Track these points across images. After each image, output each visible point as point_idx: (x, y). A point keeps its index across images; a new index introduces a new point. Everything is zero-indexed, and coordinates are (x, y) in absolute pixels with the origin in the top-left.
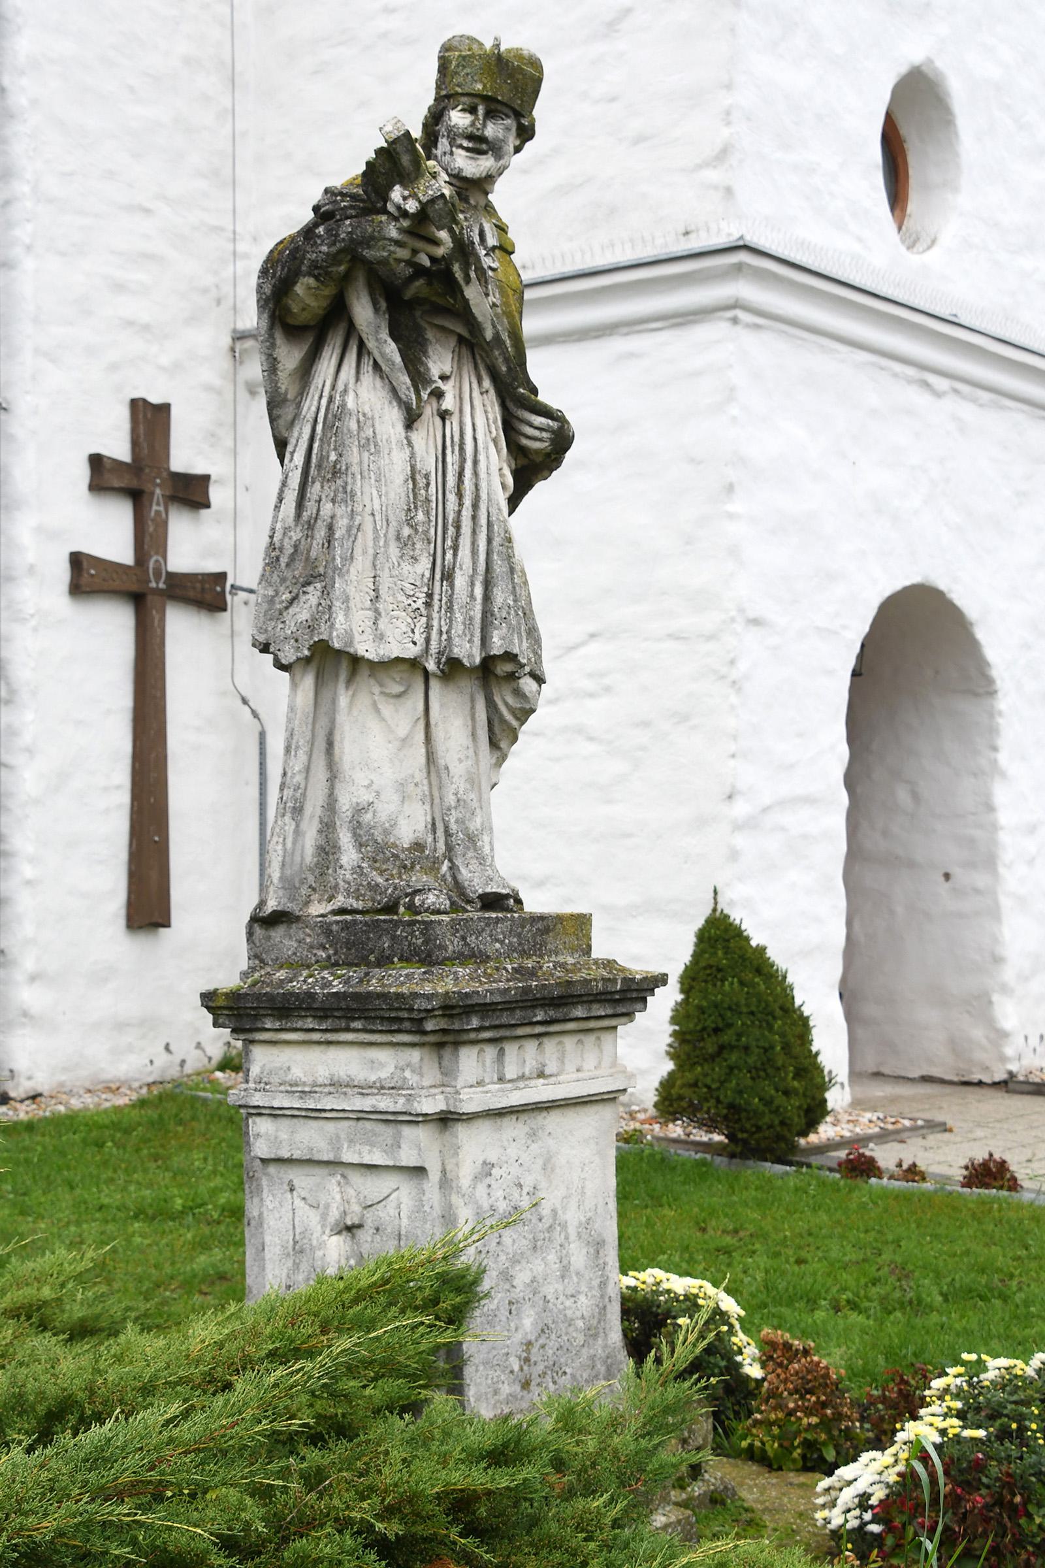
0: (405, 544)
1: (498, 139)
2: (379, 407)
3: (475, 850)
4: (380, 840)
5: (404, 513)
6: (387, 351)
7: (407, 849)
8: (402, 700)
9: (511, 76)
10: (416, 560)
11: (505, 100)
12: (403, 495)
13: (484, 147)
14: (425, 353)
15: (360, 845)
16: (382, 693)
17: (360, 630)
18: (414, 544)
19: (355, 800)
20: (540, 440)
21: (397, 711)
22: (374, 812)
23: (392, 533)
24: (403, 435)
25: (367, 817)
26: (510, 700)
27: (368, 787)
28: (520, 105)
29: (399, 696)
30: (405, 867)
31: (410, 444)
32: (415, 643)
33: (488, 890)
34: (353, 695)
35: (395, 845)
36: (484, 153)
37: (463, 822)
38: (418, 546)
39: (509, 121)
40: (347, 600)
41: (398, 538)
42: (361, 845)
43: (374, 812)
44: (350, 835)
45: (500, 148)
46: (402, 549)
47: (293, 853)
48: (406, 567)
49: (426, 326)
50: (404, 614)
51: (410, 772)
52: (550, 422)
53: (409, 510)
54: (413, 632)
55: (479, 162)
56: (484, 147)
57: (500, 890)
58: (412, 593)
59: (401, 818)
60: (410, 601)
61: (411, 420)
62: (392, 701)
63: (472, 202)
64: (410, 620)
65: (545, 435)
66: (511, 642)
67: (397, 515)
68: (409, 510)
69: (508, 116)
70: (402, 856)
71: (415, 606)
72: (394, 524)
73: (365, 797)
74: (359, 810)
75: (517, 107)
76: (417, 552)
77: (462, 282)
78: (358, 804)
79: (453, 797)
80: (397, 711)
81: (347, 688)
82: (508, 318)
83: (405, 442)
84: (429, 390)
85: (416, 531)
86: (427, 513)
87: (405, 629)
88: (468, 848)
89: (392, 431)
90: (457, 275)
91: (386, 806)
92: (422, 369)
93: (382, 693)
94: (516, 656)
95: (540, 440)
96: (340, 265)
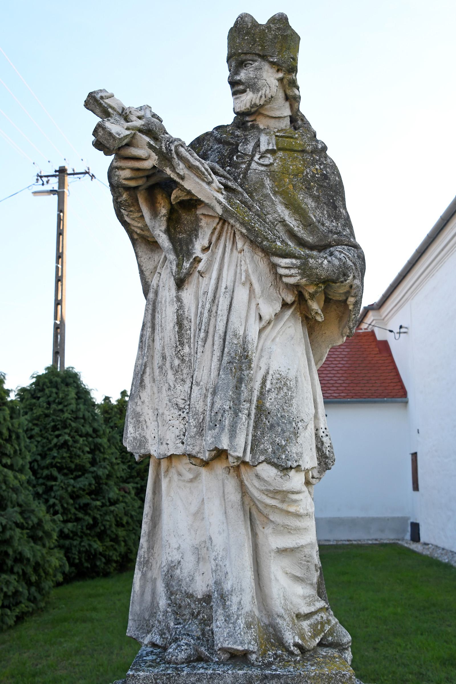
0: (177, 371)
1: (251, 79)
2: (164, 280)
3: (224, 608)
4: (183, 592)
5: (173, 349)
6: (161, 241)
7: (199, 600)
8: (195, 484)
9: (247, 34)
10: (184, 381)
11: (245, 50)
12: (173, 337)
13: (241, 87)
14: (197, 236)
15: (170, 593)
16: (179, 480)
17: (153, 436)
18: (182, 370)
19: (170, 559)
20: (291, 276)
21: (191, 493)
22: (181, 569)
23: (168, 364)
24: (175, 295)
25: (178, 572)
26: (256, 483)
27: (178, 548)
28: (261, 50)
29: (191, 481)
30: (193, 614)
31: (179, 299)
32: (183, 443)
33: (225, 645)
34: (170, 481)
35: (190, 596)
36: (244, 91)
37: (220, 584)
38: (185, 371)
39: (257, 64)
40: (137, 415)
41: (172, 368)
42: (172, 594)
43: (181, 569)
44: (164, 585)
45: (254, 84)
46: (175, 375)
47: (143, 594)
48: (179, 388)
49: (201, 217)
50: (178, 422)
51: (203, 539)
52: (294, 261)
53: (177, 347)
54: (184, 435)
55: (242, 99)
56: (241, 87)
57: (235, 647)
58: (183, 406)
59: (197, 574)
60: (181, 413)
61: (180, 283)
62: (188, 485)
63: (261, 127)
64: (182, 426)
65: (293, 271)
66: (220, 441)
67: (169, 352)
68: (177, 347)
69: (254, 61)
70: (193, 606)
71: (183, 415)
72: (168, 359)
73: (176, 556)
74: (172, 567)
75: (257, 52)
76: (185, 376)
77: (178, 180)
78: (172, 562)
79: (213, 562)
80: (191, 493)
81: (165, 476)
82: (281, 194)
83: (175, 299)
84: (191, 260)
85: (183, 361)
86: (189, 347)
87: (178, 434)
88: (218, 606)
89: (168, 294)
90: (172, 176)
91: (187, 564)
92: (190, 248)
93: (179, 480)
94: (227, 450)
95: (291, 276)
96: (122, 196)
